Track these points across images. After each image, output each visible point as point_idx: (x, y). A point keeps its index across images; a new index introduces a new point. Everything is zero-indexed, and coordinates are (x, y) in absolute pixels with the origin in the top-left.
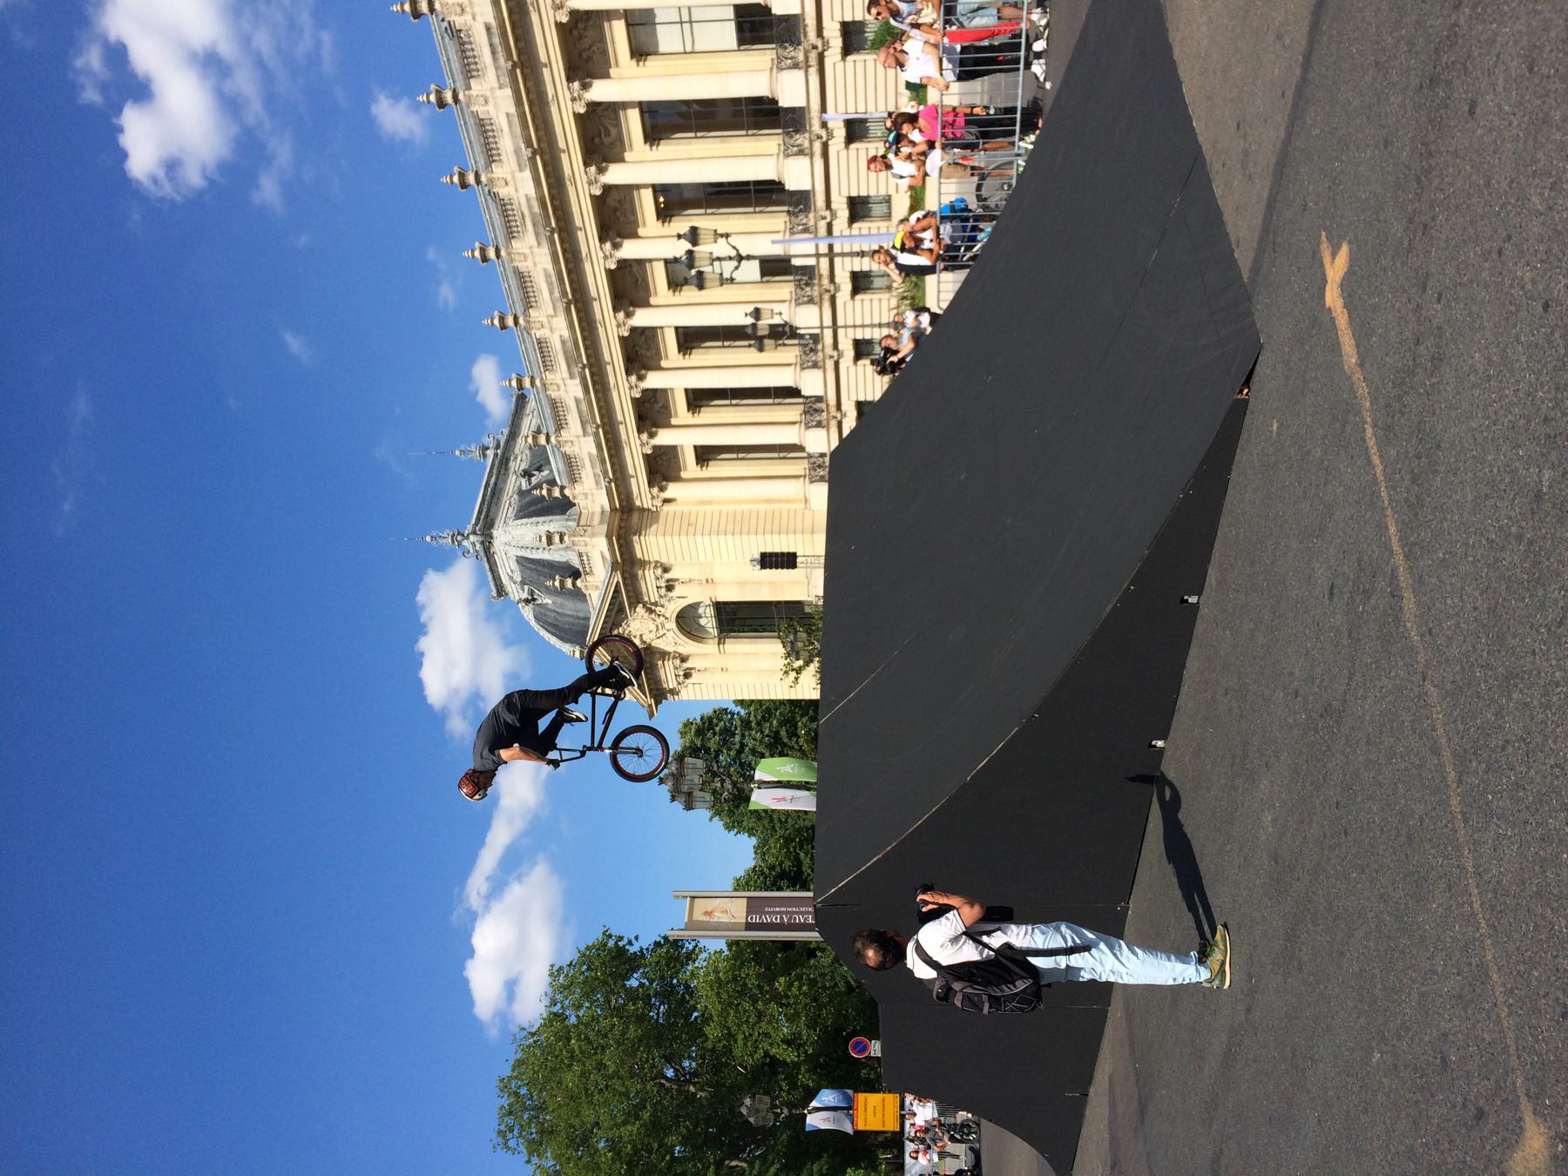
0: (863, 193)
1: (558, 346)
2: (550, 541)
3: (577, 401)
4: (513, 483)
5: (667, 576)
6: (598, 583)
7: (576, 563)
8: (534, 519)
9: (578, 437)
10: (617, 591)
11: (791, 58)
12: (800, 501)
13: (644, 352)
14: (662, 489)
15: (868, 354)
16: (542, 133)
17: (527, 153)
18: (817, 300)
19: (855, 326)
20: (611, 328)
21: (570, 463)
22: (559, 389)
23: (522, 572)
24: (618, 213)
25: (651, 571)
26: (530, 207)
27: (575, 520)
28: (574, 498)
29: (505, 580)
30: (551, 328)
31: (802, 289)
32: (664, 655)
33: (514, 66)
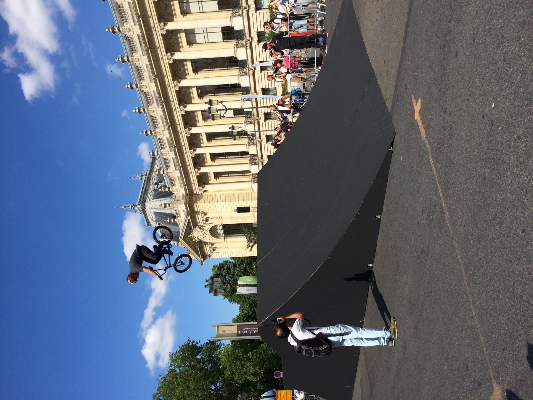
0: (267, 87)
1: (166, 141)
2: (165, 206)
3: (173, 159)
4: (152, 187)
5: (206, 216)
6: (182, 220)
7: (174, 213)
8: (160, 199)
9: (174, 171)
10: (189, 222)
11: (241, 44)
12: (250, 189)
13: (195, 142)
14: (203, 187)
15: (271, 140)
16: (158, 70)
17: (153, 77)
18: (253, 122)
19: (266, 131)
20: (184, 134)
21: (171, 180)
22: (167, 155)
23: (156, 217)
24: (185, 96)
25: (200, 215)
26: (155, 95)
27: (173, 199)
28: (173, 191)
29: (150, 220)
30: (163, 135)
31: (248, 119)
32: (206, 243)
33: (148, 48)
